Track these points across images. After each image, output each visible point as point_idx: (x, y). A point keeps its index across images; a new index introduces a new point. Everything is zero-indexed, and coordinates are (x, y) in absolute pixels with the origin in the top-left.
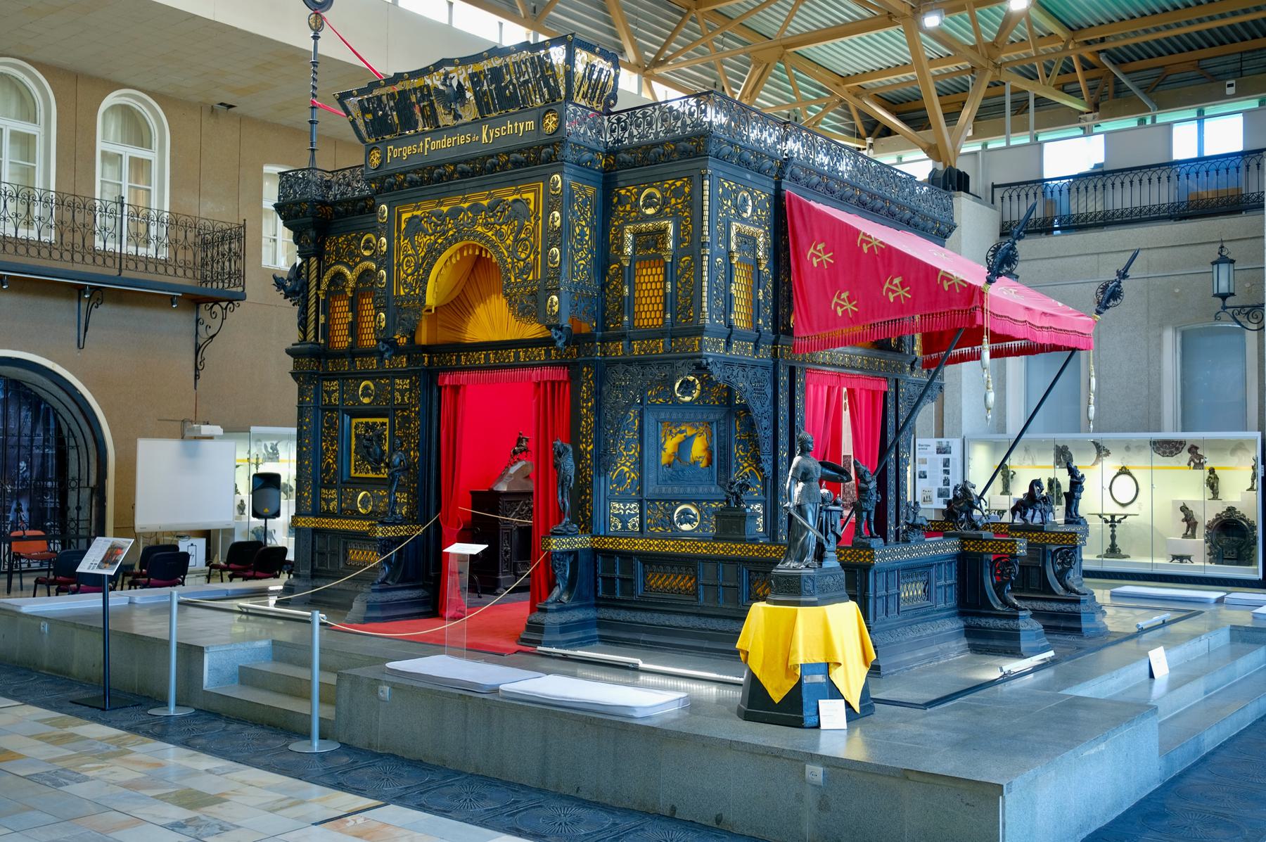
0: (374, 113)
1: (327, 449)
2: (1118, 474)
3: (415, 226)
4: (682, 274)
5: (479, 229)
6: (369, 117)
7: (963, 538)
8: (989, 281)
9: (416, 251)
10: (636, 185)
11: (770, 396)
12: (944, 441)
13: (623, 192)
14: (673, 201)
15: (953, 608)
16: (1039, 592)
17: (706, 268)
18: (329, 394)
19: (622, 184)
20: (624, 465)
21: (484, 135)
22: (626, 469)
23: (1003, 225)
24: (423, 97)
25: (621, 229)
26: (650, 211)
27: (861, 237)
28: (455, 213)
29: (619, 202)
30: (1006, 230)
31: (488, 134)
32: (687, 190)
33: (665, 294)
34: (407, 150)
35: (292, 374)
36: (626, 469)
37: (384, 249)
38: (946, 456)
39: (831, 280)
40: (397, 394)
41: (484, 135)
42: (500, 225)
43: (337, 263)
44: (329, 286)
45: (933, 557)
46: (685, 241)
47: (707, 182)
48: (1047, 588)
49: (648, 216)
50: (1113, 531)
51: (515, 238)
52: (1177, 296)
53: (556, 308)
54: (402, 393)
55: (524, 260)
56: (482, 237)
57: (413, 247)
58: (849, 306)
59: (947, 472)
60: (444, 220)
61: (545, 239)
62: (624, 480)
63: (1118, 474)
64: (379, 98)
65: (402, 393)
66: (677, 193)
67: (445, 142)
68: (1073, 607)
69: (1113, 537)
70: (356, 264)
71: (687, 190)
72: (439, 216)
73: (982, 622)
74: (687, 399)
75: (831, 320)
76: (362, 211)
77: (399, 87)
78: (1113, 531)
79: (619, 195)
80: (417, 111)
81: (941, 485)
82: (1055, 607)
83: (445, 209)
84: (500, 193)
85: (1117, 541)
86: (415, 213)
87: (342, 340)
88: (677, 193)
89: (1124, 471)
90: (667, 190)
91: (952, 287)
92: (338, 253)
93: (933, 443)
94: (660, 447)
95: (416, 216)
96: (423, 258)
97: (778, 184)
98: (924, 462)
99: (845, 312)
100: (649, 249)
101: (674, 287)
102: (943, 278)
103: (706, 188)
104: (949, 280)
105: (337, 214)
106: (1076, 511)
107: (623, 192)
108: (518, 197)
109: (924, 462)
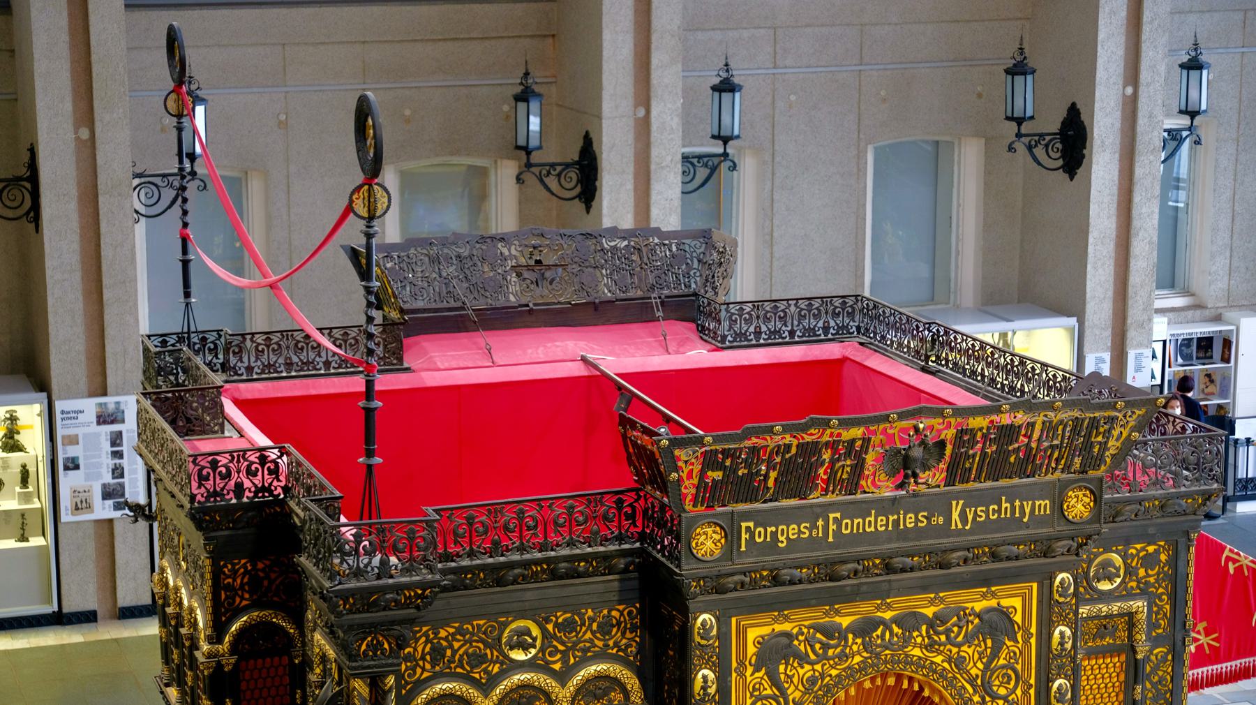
5: (917, 652)
9: (783, 693)
12: (110, 401)
14: (1142, 572)
26: (1105, 586)
27: (1226, 553)
28: (865, 628)
31: (963, 516)
32: (1163, 557)
41: (955, 515)
42: (959, 645)
46: (1159, 627)
51: (987, 666)
52: (407, 121)
56: (920, 664)
57: (775, 682)
58: (1203, 640)
59: (118, 455)
67: (877, 523)
70: (494, 681)
71: (1163, 557)
72: (829, 631)
81: (108, 478)
83: (845, 622)
84: (953, 597)
86: (778, 628)
90: (1133, 556)
92: (437, 653)
93: (89, 406)
98: (73, 440)
99: (1200, 648)
100: (1102, 638)
108: (993, 603)
109: (73, 440)
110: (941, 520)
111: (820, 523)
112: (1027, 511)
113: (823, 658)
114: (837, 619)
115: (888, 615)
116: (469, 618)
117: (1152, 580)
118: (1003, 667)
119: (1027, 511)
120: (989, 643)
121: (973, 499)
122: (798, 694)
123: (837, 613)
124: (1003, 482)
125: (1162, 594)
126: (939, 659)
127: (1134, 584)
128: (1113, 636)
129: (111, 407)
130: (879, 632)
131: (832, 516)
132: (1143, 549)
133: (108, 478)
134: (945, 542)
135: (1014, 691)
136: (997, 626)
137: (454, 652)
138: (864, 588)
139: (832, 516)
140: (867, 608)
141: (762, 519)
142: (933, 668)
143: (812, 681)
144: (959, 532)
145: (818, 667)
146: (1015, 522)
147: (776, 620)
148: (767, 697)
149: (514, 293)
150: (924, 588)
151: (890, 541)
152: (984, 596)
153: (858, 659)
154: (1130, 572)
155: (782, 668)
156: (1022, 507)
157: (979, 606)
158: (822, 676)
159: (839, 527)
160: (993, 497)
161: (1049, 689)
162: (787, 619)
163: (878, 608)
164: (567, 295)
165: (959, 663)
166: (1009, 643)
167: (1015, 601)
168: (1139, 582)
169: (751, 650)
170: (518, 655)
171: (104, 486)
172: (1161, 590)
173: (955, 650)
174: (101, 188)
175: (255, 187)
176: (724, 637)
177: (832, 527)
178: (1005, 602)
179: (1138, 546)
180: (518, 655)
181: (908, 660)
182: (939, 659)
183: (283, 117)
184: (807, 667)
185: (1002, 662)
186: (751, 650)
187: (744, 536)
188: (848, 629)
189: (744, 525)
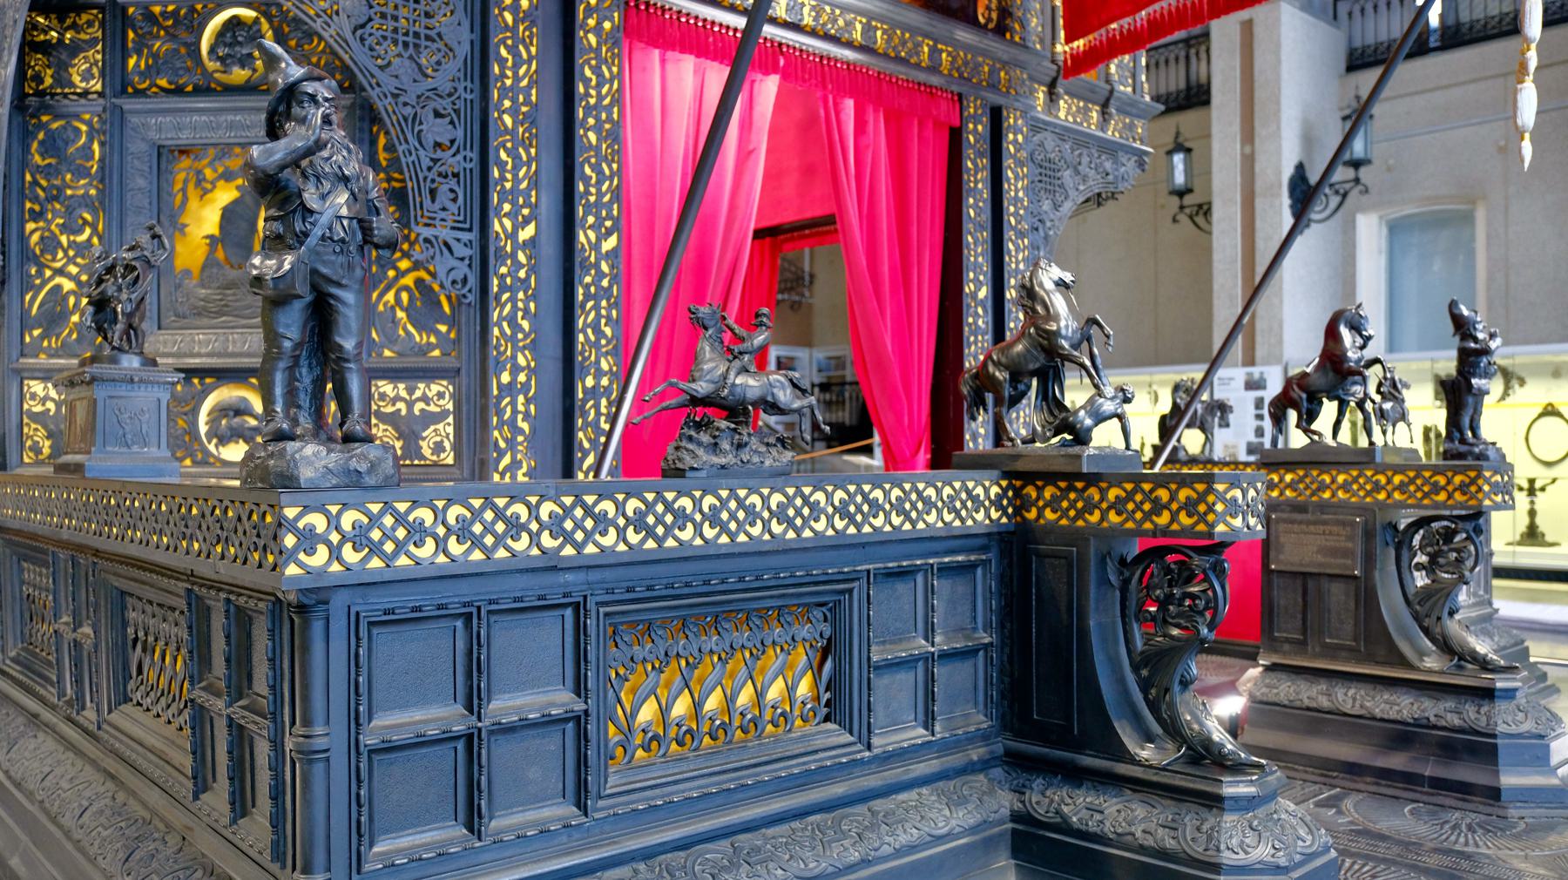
2: (1541, 415)
7: (1022, 479)
12: (1256, 371)
15: (984, 737)
16: (1354, 654)
20: (60, 272)
22: (68, 285)
30: (1356, 62)
36: (68, 285)
38: (1259, 393)
45: (840, 545)
48: (1374, 639)
50: (1532, 502)
62: (64, 315)
63: (1541, 415)
68: (1473, 714)
69: (1532, 513)
73: (1079, 807)
74: (239, 75)
78: (1532, 502)
81: (1252, 438)
82: (1404, 706)
85: (1538, 521)
89: (1550, 411)
94: (167, 219)
106: (1474, 429)
129: (1256, 376)
133: (1252, 438)
171: (1249, 444)
175: (1481, 215)
183: (1502, 143)
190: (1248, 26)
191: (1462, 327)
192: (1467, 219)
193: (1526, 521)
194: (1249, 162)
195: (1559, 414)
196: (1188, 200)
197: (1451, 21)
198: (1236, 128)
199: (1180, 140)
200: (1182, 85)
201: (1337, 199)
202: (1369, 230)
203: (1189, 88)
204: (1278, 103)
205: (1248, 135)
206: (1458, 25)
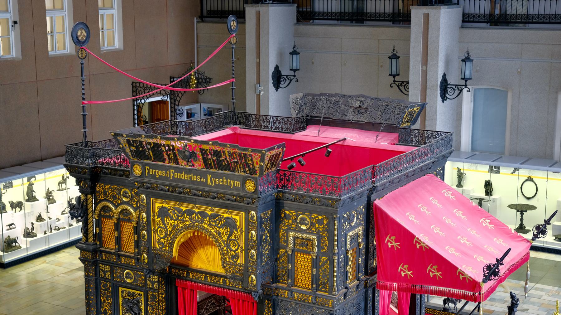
0: (136, 147)
1: (104, 301)
2: (526, 180)
3: (163, 213)
4: (323, 264)
5: (206, 226)
6: (133, 148)
8: (484, 281)
9: (166, 227)
10: (296, 211)
11: (363, 308)
13: (287, 212)
17: (336, 266)
18: (105, 272)
19: (287, 208)
21: (209, 180)
23: (464, 15)
24: (169, 149)
25: (287, 232)
26: (303, 227)
27: (415, 239)
28: (190, 213)
29: (285, 217)
31: (211, 180)
32: (325, 222)
33: (313, 275)
34: (159, 173)
35: (81, 260)
37: (145, 220)
39: (397, 257)
40: (149, 283)
41: (209, 180)
43: (105, 200)
44: (100, 211)
46: (324, 249)
47: (336, 222)
49: (302, 229)
50: (522, 216)
51: (228, 237)
53: (255, 283)
54: (153, 283)
55: (234, 251)
57: (164, 223)
60: (183, 214)
61: (247, 245)
64: (141, 142)
65: (153, 283)
66: (320, 222)
67: (185, 177)
69: (522, 220)
72: (180, 211)
75: (396, 277)
76: (121, 176)
77: (155, 140)
78: (522, 216)
79: (285, 214)
80: (165, 154)
83: (184, 209)
84: (218, 210)
85: (524, 222)
86: (164, 205)
87: (110, 243)
88: (320, 222)
89: (530, 179)
90: (313, 219)
91: (464, 278)
95: (165, 208)
96: (171, 232)
97: (369, 198)
101: (318, 271)
102: (460, 273)
103: (336, 224)
104: (463, 275)
105: (105, 173)
107: (287, 212)
108: (230, 216)
110: (204, 180)
111: (168, 172)
112: (232, 184)
113: (177, 219)
114: (181, 208)
115: (197, 211)
116: (113, 184)
117: (321, 230)
118: (233, 240)
119: (232, 184)
120: (229, 230)
121: (214, 176)
122: (170, 229)
123: (181, 205)
124: (225, 172)
125: (325, 236)
126: (213, 231)
127: (314, 229)
128: (306, 247)
130: (194, 215)
131: (171, 170)
132: (317, 217)
134: (206, 188)
135: (237, 250)
136: (230, 224)
137: (109, 194)
138: (188, 199)
139: (171, 170)
140: (190, 206)
141: (153, 167)
142: (211, 234)
143: (174, 227)
144: (211, 186)
145: (176, 222)
146: (228, 187)
147: (163, 203)
148: (161, 227)
149: (351, 116)
150: (207, 204)
151: (189, 183)
152: (227, 213)
153: (187, 223)
154: (312, 224)
155: (165, 219)
156: (230, 182)
157: (226, 216)
158: (178, 225)
159: (174, 175)
160: (220, 177)
161: (249, 253)
162: (166, 203)
163: (194, 207)
164: (364, 118)
165: (219, 234)
166: (235, 232)
167: (238, 217)
168: (316, 229)
169: (157, 210)
170: (124, 199)
172: (324, 235)
173: (218, 229)
174: (428, 86)
175: (510, 94)
176: (148, 203)
177: (172, 175)
178: (234, 217)
179: (316, 215)
180: (124, 199)
181: (203, 228)
182: (213, 231)
183: (519, 70)
184: (173, 221)
185: (233, 238)
186: (157, 210)
187: (147, 171)
188: (185, 211)
189: (147, 167)
190: (427, 16)
191: (513, 297)
192: (505, 94)
193: (520, 223)
194: (425, 74)
195: (533, 181)
196: (397, 78)
197: (503, 11)
198: (420, 58)
199: (395, 53)
200: (391, 11)
201: (457, 92)
202: (467, 96)
203: (394, 13)
204: (438, 52)
205: (425, 62)
206: (506, 15)
